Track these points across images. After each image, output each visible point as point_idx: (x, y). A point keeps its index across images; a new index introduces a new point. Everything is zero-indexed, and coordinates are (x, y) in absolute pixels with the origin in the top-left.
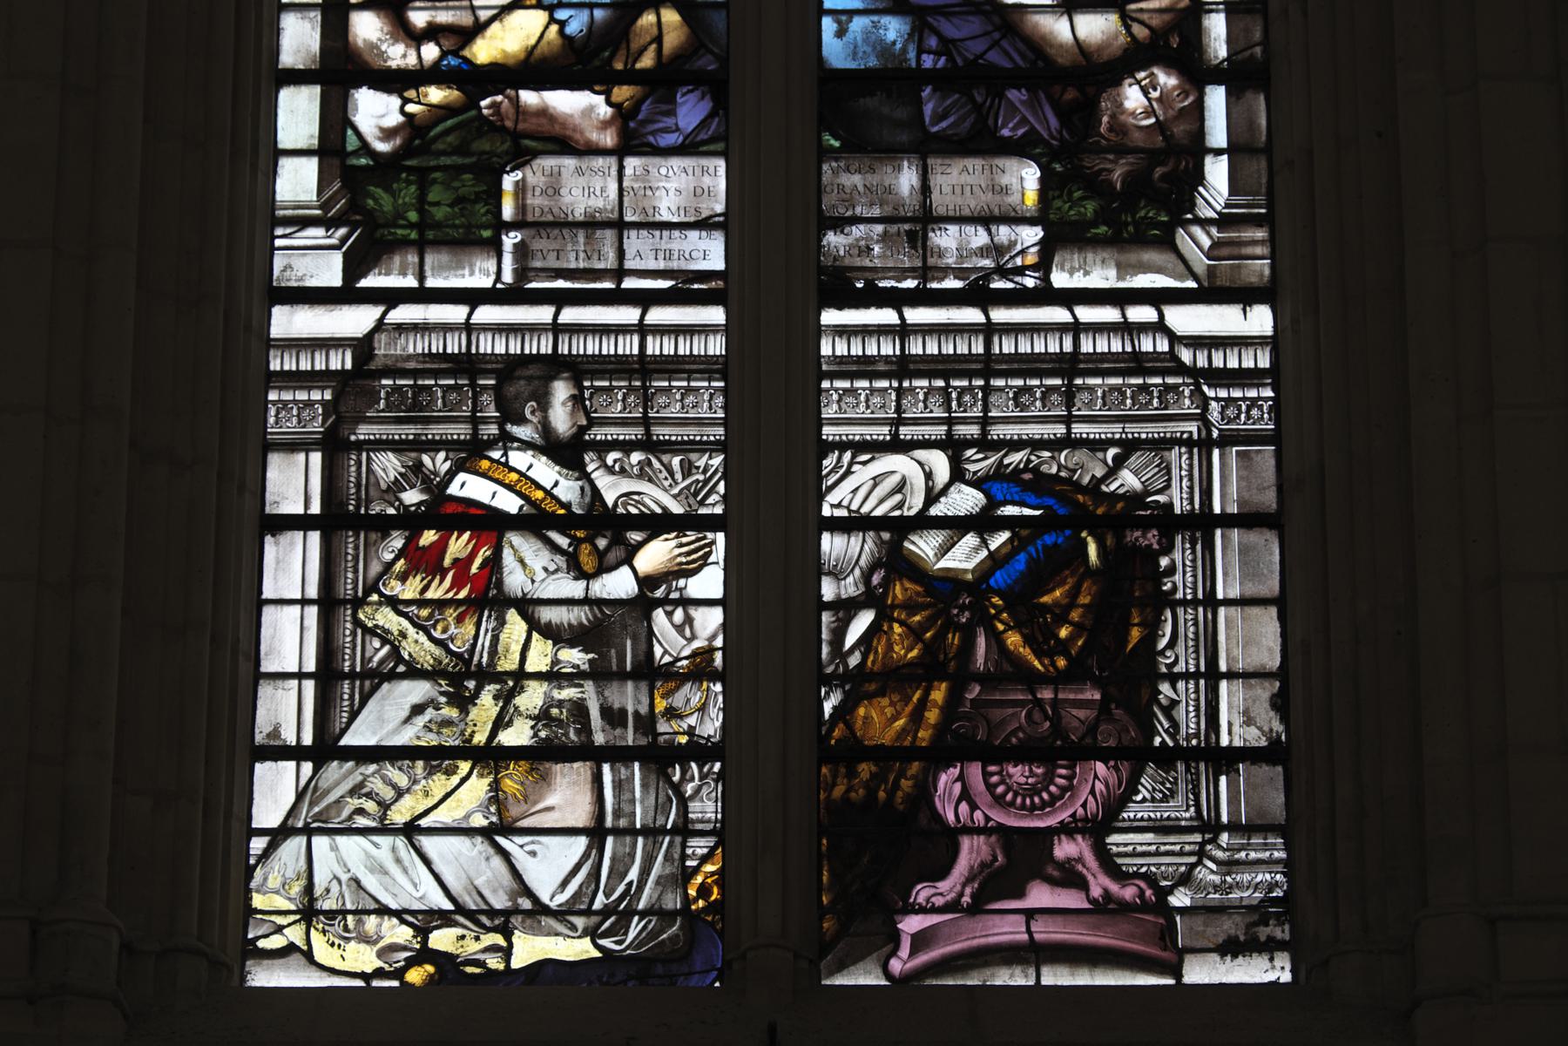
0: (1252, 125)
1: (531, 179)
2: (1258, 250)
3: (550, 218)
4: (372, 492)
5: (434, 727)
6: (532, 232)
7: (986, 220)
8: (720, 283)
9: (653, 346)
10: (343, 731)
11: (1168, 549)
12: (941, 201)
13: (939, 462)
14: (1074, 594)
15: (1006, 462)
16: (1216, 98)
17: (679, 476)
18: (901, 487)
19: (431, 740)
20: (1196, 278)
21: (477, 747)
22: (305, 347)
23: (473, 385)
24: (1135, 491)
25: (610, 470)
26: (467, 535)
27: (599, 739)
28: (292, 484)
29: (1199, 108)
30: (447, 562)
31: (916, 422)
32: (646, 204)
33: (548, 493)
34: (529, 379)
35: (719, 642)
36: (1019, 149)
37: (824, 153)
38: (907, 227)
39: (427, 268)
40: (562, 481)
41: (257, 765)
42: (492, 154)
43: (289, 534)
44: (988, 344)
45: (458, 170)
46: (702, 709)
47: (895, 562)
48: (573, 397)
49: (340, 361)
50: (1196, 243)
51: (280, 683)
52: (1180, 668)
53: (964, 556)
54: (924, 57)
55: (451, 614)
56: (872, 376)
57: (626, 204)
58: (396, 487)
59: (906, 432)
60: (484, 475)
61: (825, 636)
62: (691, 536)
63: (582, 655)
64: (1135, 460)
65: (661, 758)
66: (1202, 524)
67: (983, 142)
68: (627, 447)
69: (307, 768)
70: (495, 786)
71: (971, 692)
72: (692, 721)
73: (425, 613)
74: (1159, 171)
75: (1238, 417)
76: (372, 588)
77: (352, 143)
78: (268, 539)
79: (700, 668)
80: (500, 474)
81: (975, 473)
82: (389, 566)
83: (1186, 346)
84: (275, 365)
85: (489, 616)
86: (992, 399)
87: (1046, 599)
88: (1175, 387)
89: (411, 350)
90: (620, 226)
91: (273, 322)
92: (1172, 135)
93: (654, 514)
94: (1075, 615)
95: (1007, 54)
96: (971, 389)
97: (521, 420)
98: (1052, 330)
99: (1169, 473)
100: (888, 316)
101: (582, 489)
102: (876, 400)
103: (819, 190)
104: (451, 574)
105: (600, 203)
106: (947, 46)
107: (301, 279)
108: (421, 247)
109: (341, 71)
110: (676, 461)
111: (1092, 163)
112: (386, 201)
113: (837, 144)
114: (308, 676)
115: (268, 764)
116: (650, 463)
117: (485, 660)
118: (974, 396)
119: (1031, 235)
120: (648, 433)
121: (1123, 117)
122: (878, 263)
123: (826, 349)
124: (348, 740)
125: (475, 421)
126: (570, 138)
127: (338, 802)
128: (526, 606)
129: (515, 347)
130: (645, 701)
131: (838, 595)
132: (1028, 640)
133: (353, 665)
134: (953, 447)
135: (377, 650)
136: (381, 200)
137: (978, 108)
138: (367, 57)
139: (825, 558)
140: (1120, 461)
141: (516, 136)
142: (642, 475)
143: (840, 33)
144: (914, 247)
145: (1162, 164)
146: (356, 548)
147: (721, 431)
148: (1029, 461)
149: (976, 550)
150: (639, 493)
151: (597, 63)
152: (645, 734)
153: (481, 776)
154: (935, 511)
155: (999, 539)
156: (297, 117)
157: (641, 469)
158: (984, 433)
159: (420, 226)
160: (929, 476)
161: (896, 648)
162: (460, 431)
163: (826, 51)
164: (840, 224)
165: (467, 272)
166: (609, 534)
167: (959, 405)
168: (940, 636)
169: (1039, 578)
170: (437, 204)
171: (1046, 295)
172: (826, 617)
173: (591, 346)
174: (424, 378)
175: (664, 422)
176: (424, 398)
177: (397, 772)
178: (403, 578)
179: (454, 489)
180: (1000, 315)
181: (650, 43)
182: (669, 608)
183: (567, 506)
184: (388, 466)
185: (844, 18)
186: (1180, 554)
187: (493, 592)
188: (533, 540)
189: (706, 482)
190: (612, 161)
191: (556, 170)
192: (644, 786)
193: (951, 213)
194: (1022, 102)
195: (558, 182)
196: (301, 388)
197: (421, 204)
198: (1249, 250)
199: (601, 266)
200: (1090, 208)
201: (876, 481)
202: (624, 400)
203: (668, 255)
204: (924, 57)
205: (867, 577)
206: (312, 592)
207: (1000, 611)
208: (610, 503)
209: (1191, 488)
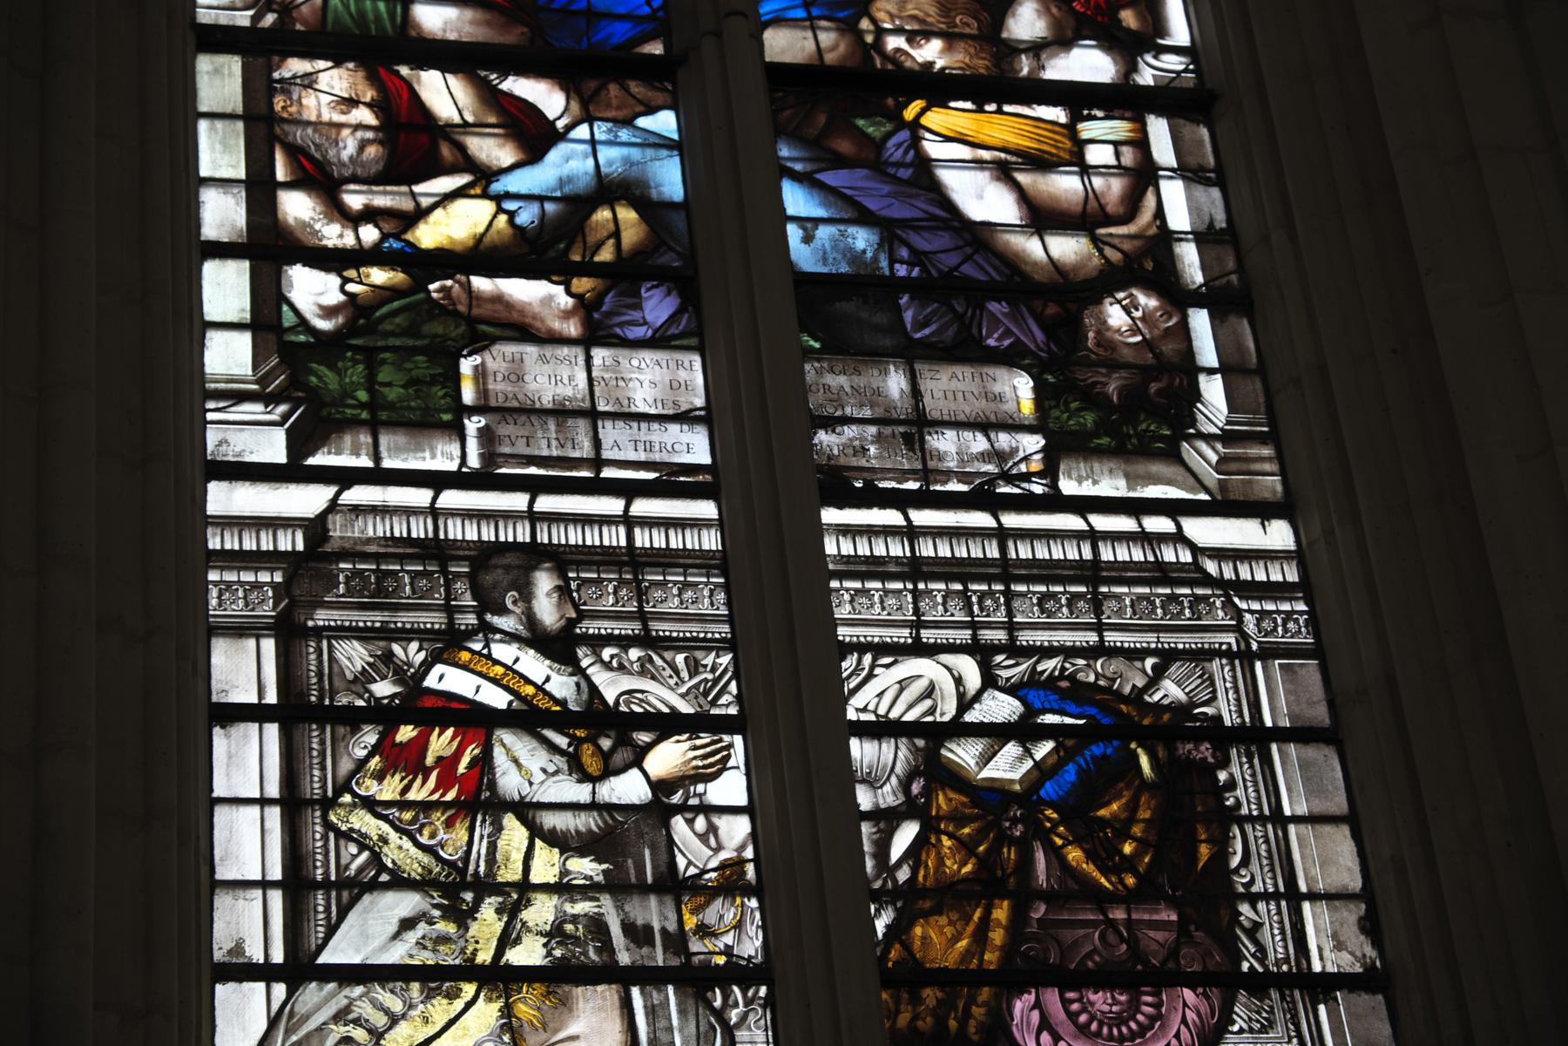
0: (1240, 347)
1: (491, 365)
2: (1267, 467)
3: (515, 404)
4: (337, 683)
5: (429, 944)
6: (498, 417)
7: (985, 426)
8: (708, 478)
9: (642, 539)
10: (320, 949)
11: (1225, 763)
12: (935, 405)
13: (969, 668)
14: (1132, 807)
15: (1040, 668)
16: (1200, 321)
17: (685, 674)
18: (930, 692)
19: (427, 958)
20: (1207, 491)
21: (482, 966)
22: (249, 526)
23: (444, 571)
24: (1180, 702)
25: (607, 666)
26: (450, 732)
27: (624, 958)
28: (241, 670)
29: (1184, 329)
30: (429, 761)
31: (937, 625)
33: (539, 688)
34: (507, 568)
35: (749, 853)
36: (1011, 358)
37: (808, 354)
38: (901, 429)
39: (383, 449)
40: (554, 675)
41: (218, 987)
42: (445, 338)
43: (242, 726)
44: (1003, 549)
45: (415, 351)
46: (739, 926)
47: (933, 771)
48: (558, 588)
49: (288, 542)
50: (1203, 457)
51: (241, 893)
52: (1258, 887)
53: (1008, 766)
55: (438, 818)
56: (885, 577)
57: (597, 394)
58: (363, 680)
59: (927, 635)
60: (465, 667)
61: (866, 848)
62: (705, 738)
63: (594, 865)
64: (1175, 669)
65: (697, 980)
66: (1255, 738)
67: (966, 349)
68: (624, 642)
69: (280, 990)
70: (507, 1012)
71: (1036, 911)
72: (729, 939)
73: (407, 816)
75: (1275, 629)
76: (344, 787)
77: (288, 319)
78: (217, 731)
79: (730, 882)
80: (483, 666)
81: (1008, 679)
82: (361, 764)
83: (1209, 557)
84: (214, 543)
85: (484, 821)
86: (1016, 604)
87: (1102, 812)
88: (1205, 598)
89: (371, 533)
91: (209, 498)
92: (1161, 353)
93: (660, 713)
94: (1137, 830)
95: (981, 268)
96: (991, 593)
97: (502, 611)
98: (1069, 537)
99: (1213, 684)
100: (892, 517)
101: (578, 685)
102: (891, 601)
103: (803, 390)
104: (435, 773)
105: (569, 392)
106: (918, 257)
108: (375, 428)
109: (269, 248)
110: (680, 659)
111: (1085, 376)
113: (817, 345)
114: (274, 884)
115: (231, 986)
116: (651, 660)
117: (482, 869)
118: (996, 601)
119: (1032, 443)
120: (646, 628)
121: (1109, 334)
122: (875, 463)
123: (830, 547)
124: (325, 958)
125: (450, 610)
126: (531, 326)
127: (319, 1029)
128: (525, 810)
129: (488, 534)
130: (673, 916)
131: (877, 804)
132: (1090, 856)
133: (326, 873)
134: (982, 653)
135: (355, 857)
136: (325, 377)
137: (960, 318)
139: (856, 765)
140: (1159, 672)
141: (471, 321)
142: (643, 673)
143: (808, 239)
144: (911, 449)
145: (1156, 380)
146: (322, 743)
147: (726, 628)
148: (1063, 669)
149: (1020, 759)
150: (643, 692)
151: (552, 254)
152: (676, 954)
153: (489, 1000)
154: (970, 717)
155: (1044, 749)
156: (225, 289)
157: (642, 666)
158: (1012, 639)
159: (370, 406)
160: (958, 681)
161: (948, 863)
162: (435, 620)
163: (794, 255)
164: (832, 423)
165: (427, 454)
166: (612, 734)
167: (982, 609)
168: (994, 850)
169: (1094, 788)
170: (389, 384)
171: (1055, 502)
172: (866, 828)
173: (574, 536)
174: (388, 563)
175: (663, 617)
176: (390, 584)
177: (389, 994)
178: (380, 777)
179: (431, 682)
180: (1011, 520)
181: (608, 238)
182: (689, 816)
183: (563, 703)
184: (353, 655)
185: (809, 225)
186: (1237, 768)
187: (485, 795)
188: (527, 739)
189: (716, 681)
190: (579, 352)
191: (517, 356)
192: (682, 1012)
193: (946, 418)
194: (1004, 314)
195: (521, 369)
196: (246, 569)
197: (371, 383)
198: (1257, 467)
199: (577, 454)
200: (1089, 419)
201: (903, 685)
202: (615, 593)
203: (649, 447)
204: (897, 266)
205: (905, 785)
206: (273, 791)
207: (1055, 825)
208: (611, 702)
209: (1238, 700)
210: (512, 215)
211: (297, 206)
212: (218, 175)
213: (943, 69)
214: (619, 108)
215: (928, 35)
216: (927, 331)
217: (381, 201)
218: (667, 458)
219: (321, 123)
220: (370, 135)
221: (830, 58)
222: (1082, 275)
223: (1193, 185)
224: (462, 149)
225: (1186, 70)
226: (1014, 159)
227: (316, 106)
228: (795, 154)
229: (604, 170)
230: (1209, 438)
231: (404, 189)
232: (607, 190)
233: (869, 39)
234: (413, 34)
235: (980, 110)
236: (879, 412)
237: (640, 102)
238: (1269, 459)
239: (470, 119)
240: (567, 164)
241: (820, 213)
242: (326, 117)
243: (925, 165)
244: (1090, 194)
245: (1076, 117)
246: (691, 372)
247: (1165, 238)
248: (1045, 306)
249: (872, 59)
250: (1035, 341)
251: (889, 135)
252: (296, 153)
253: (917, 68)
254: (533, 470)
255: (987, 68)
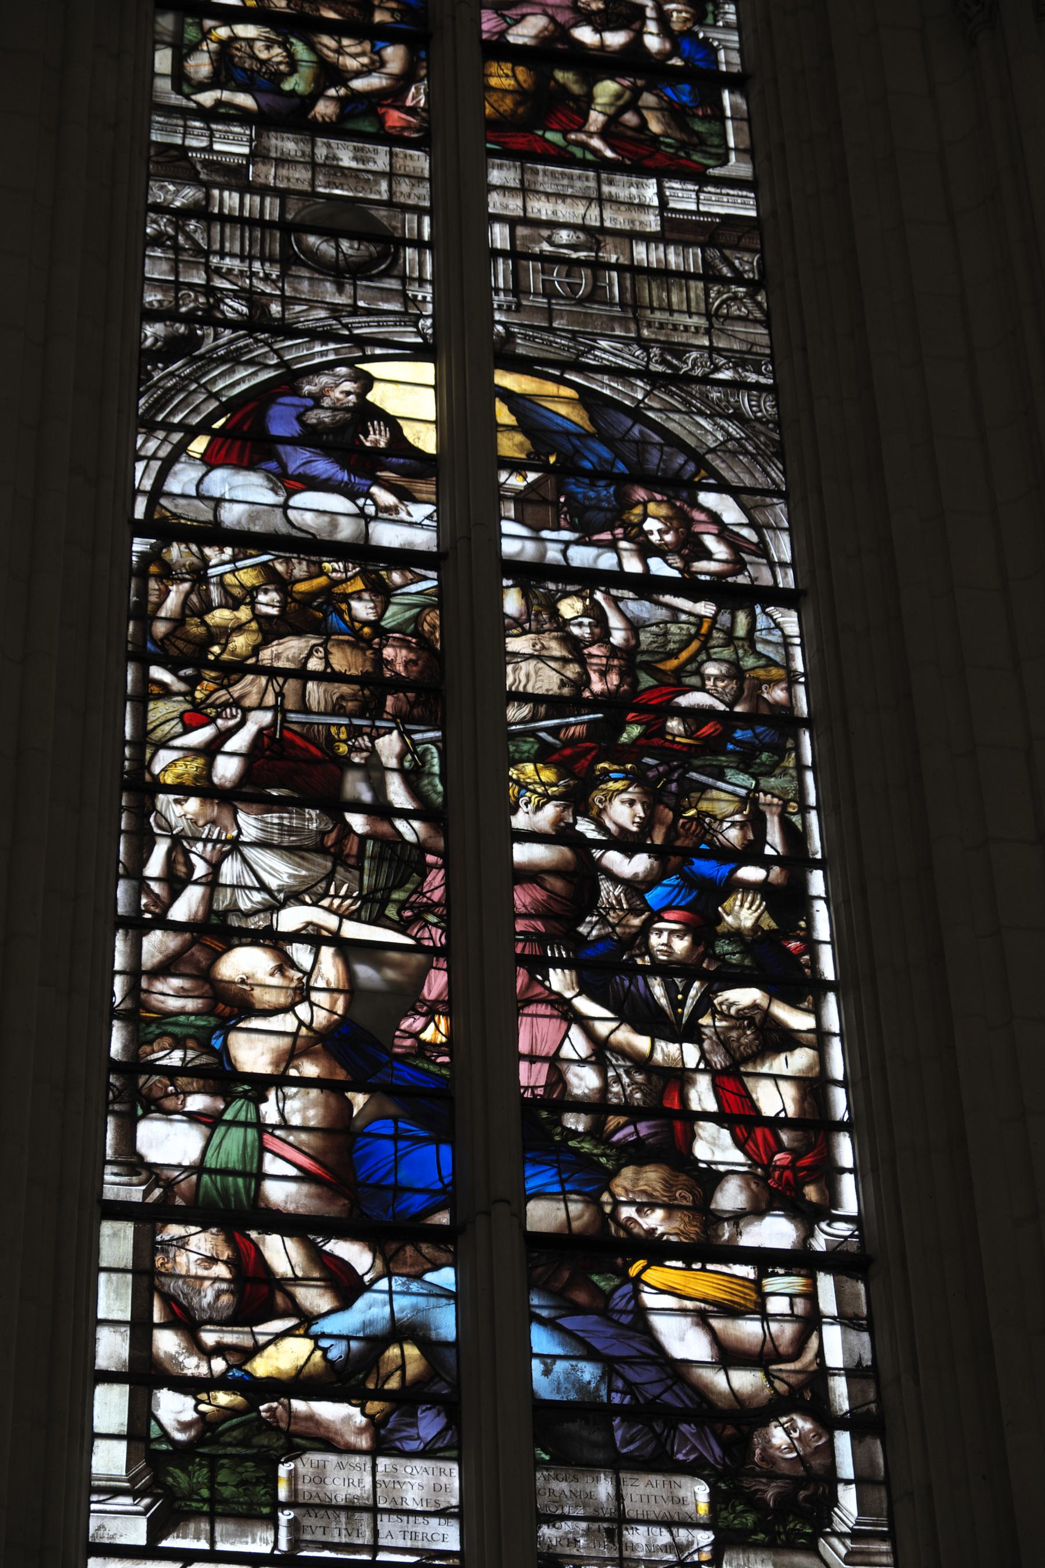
0: (872, 1463)
1: (301, 1470)
3: (317, 1501)
6: (303, 1511)
7: (669, 1524)
8: (457, 1561)
12: (632, 1507)
16: (843, 1441)
29: (830, 1448)
32: (395, 1494)
36: (693, 1470)
37: (539, 1464)
38: (605, 1525)
42: (269, 1447)
54: (613, 1394)
67: (662, 1463)
74: (802, 1494)
77: (155, 1431)
90: (374, 1510)
92: (811, 1467)
103: (534, 1493)
105: (358, 1492)
106: (630, 1388)
107: (112, 1537)
108: (212, 1518)
111: (750, 1484)
112: (183, 1479)
113: (547, 1458)
119: (704, 1538)
121: (771, 1451)
122: (583, 1552)
126: (333, 1440)
137: (657, 1436)
138: (167, 1365)
141: (289, 1435)
143: (547, 1372)
144: (612, 1541)
145: (804, 1489)
151: (353, 1382)
156: (110, 1407)
159: (211, 1501)
163: (536, 1385)
164: (553, 1520)
170: (225, 1484)
190: (367, 1460)
191: (321, 1463)
193: (640, 1517)
194: (693, 1435)
195: (324, 1473)
199: (360, 1541)
200: (750, 1519)
203: (414, 1536)
204: (613, 1394)
210: (325, 1351)
211: (167, 1342)
212: (111, 1317)
213: (663, 1234)
214: (412, 1265)
215: (653, 1206)
216: (631, 1447)
217: (229, 1339)
218: (427, 1545)
219: (189, 1276)
220: (224, 1286)
221: (576, 1225)
222: (755, 1404)
223: (848, 1330)
224: (292, 1297)
225: (852, 1236)
226: (711, 1308)
227: (186, 1262)
228: (543, 1303)
229: (397, 1315)
230: (840, 1536)
231: (247, 1329)
232: (400, 1331)
233: (608, 1209)
234: (262, 1205)
235: (688, 1268)
236: (590, 1512)
237: (429, 1260)
238: (886, 1553)
239: (300, 1274)
240: (370, 1310)
241: (558, 1351)
242: (193, 1272)
243: (642, 1312)
244: (768, 1337)
245: (762, 1274)
246: (450, 1478)
247: (822, 1372)
248: (724, 1428)
249: (609, 1226)
250: (714, 1456)
251: (616, 1288)
252: (169, 1300)
253: (642, 1233)
254: (327, 1554)
255: (697, 1233)
